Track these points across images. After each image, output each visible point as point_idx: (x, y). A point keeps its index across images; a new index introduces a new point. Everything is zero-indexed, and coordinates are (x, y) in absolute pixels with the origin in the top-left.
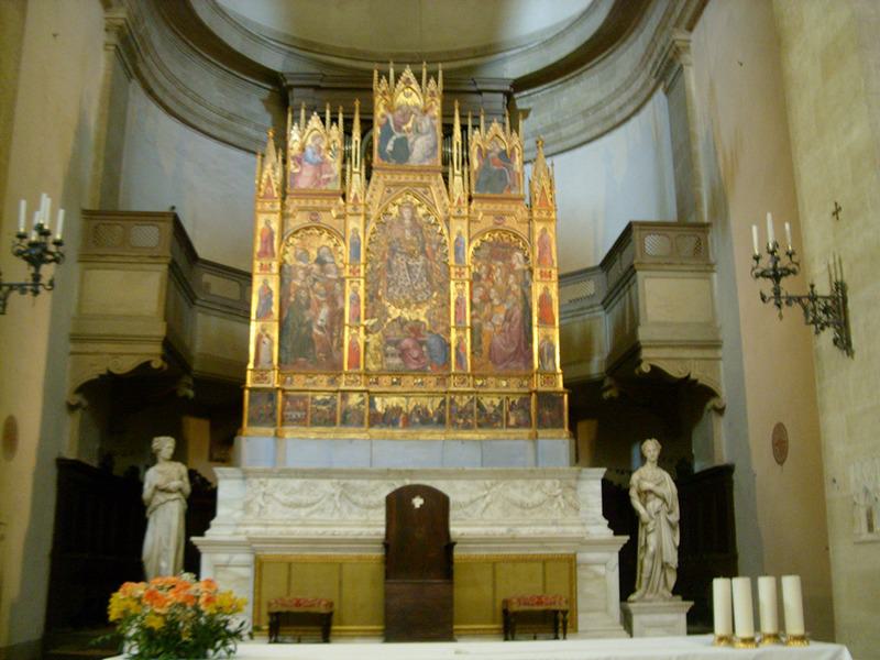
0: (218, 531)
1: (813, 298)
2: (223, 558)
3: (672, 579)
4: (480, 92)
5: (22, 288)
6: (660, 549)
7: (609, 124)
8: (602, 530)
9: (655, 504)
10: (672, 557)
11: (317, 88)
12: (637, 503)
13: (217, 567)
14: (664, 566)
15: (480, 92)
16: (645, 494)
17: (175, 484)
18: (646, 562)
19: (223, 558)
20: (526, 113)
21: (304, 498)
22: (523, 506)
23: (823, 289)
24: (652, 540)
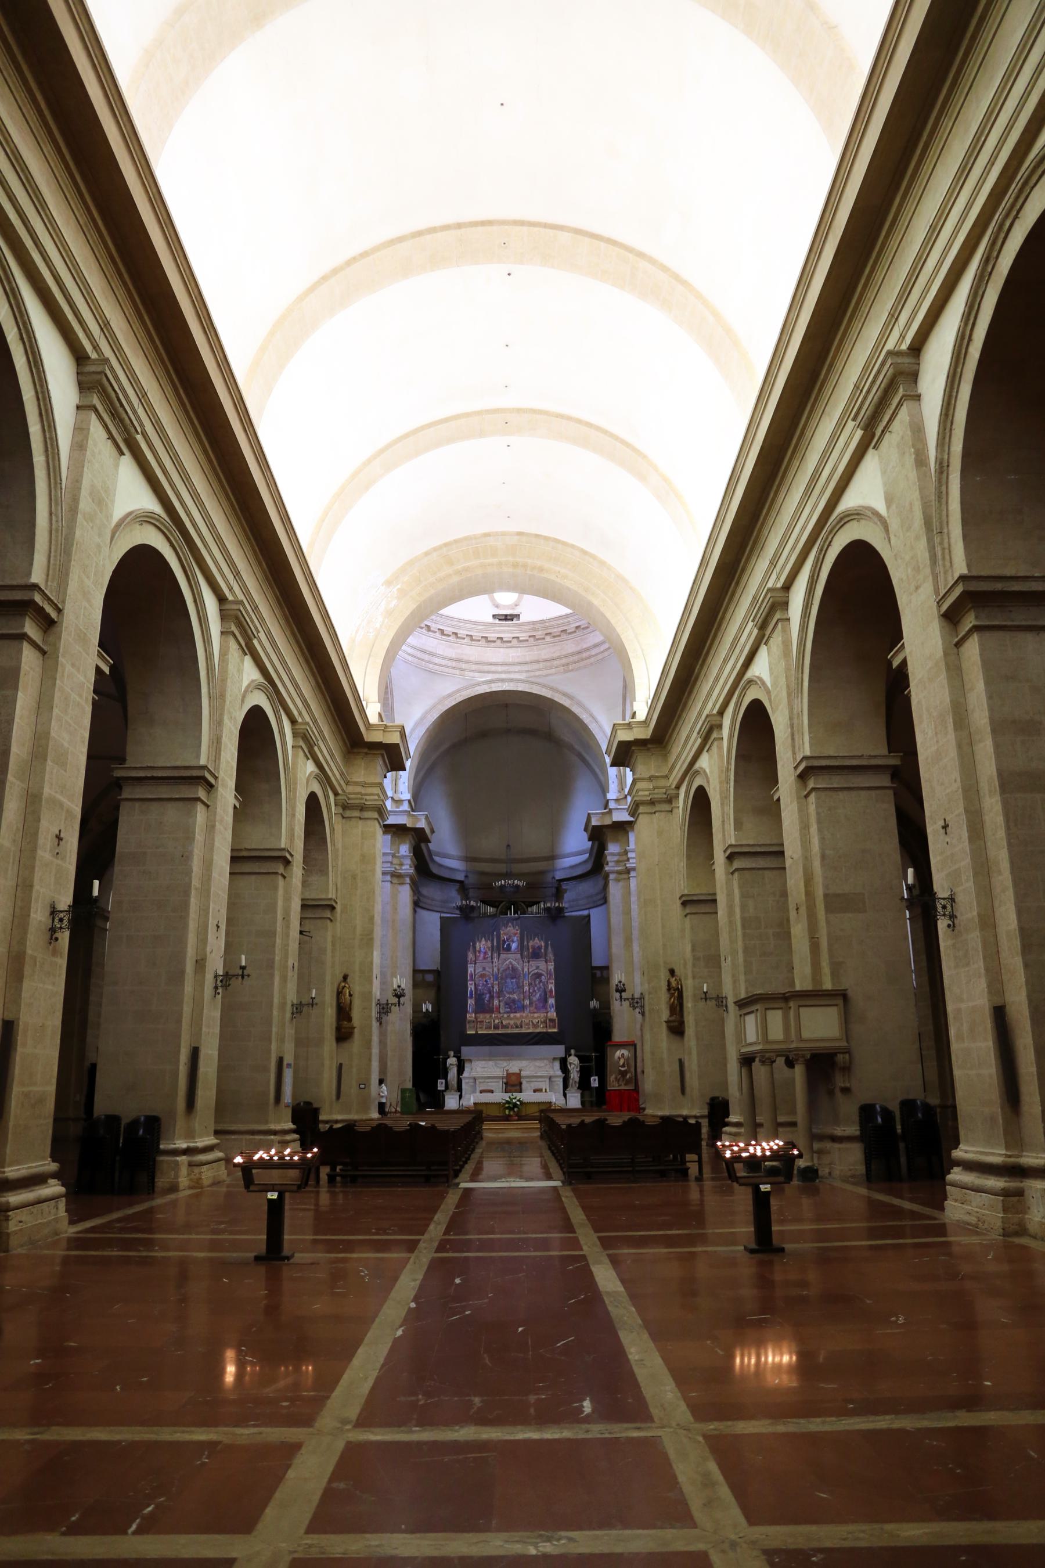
0: (465, 1074)
1: (633, 999)
2: (467, 1081)
3: (577, 1085)
4: (545, 888)
5: (395, 1005)
6: (574, 1078)
7: (595, 905)
8: (559, 1073)
9: (573, 1066)
10: (577, 1079)
11: (479, 888)
12: (569, 1066)
13: (466, 1083)
14: (575, 1082)
15: (545, 888)
16: (570, 1064)
17: (455, 1063)
18: (571, 1081)
19: (467, 1081)
20: (566, 891)
21: (486, 1066)
22: (539, 1067)
23: (637, 995)
24: (572, 1075)
